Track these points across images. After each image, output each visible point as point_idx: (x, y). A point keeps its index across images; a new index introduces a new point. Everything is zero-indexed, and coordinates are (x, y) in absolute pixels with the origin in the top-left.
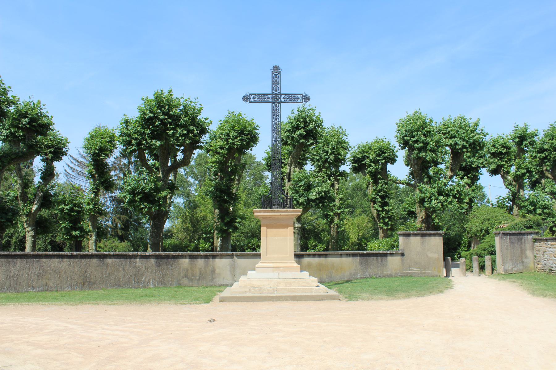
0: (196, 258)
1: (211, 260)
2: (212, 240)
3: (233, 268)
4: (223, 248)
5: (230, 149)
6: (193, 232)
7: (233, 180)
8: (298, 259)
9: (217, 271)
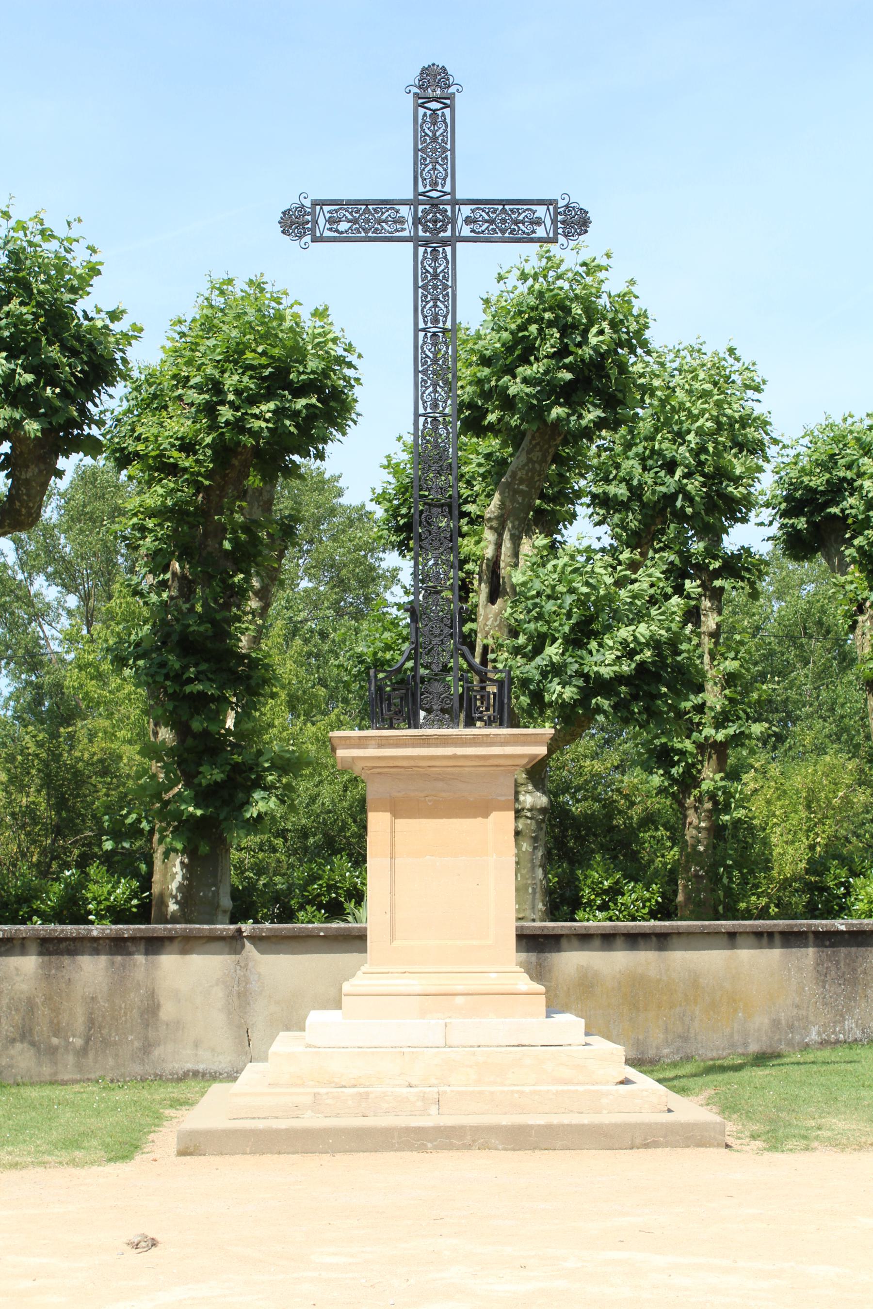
0: (72, 952)
1: (140, 959)
2: (143, 867)
3: (241, 997)
4: (194, 904)
5: (223, 452)
6: (58, 831)
7: (239, 594)
8: (533, 957)
9: (168, 1011)
